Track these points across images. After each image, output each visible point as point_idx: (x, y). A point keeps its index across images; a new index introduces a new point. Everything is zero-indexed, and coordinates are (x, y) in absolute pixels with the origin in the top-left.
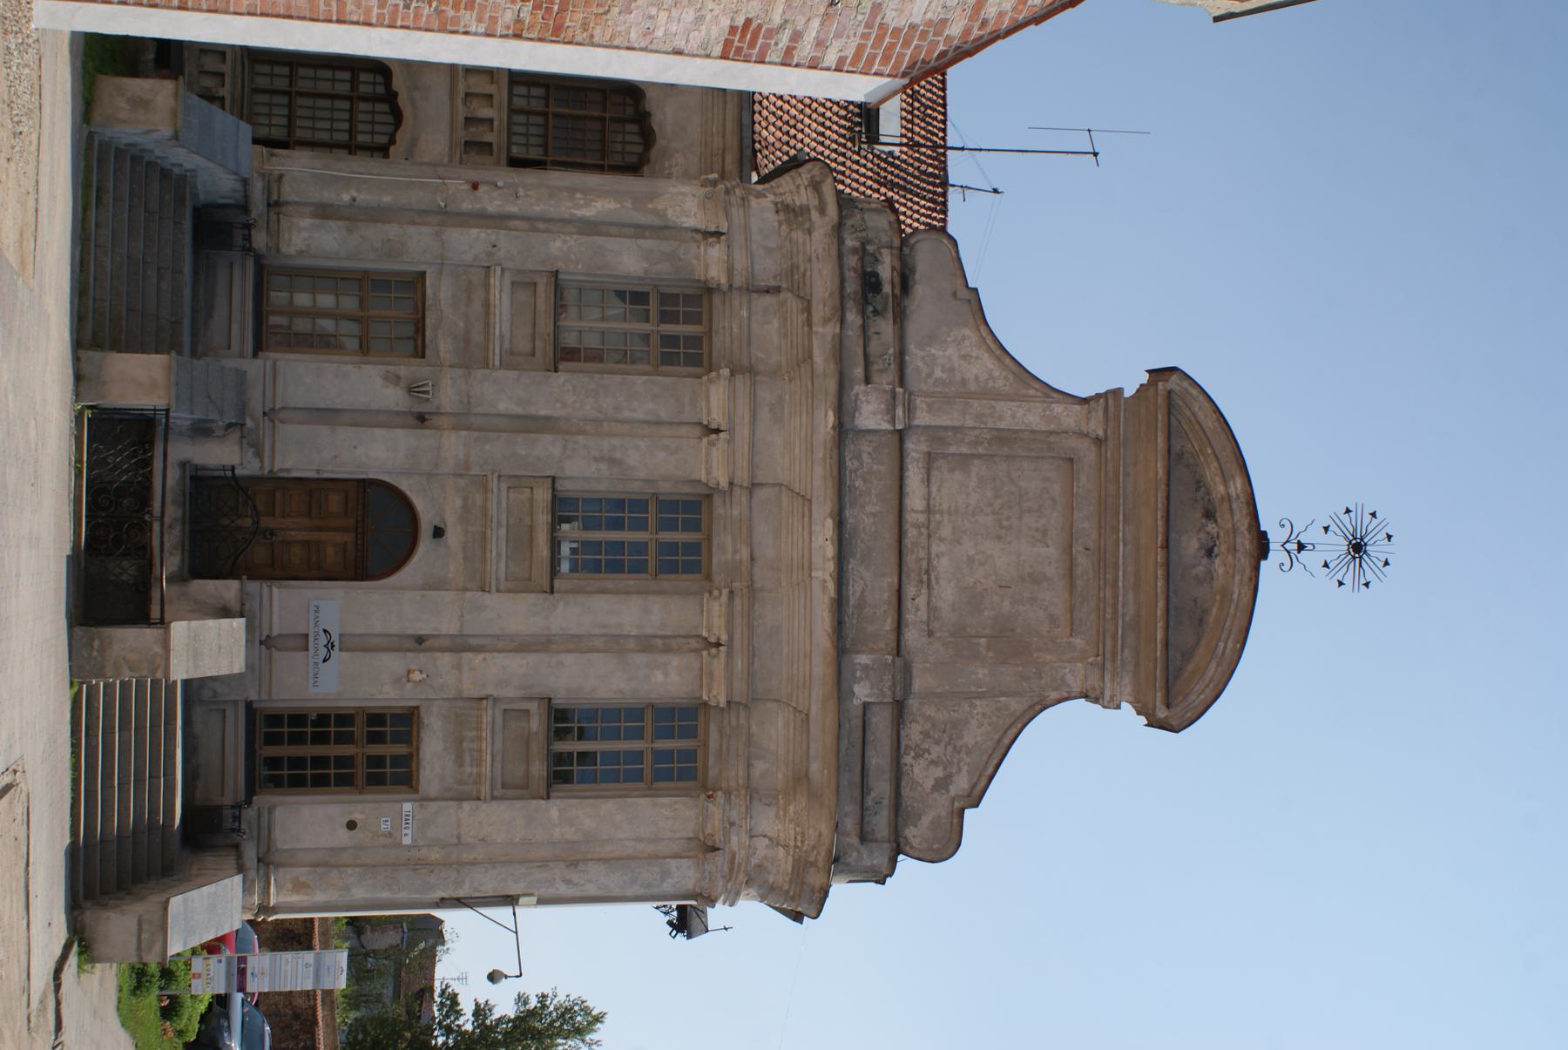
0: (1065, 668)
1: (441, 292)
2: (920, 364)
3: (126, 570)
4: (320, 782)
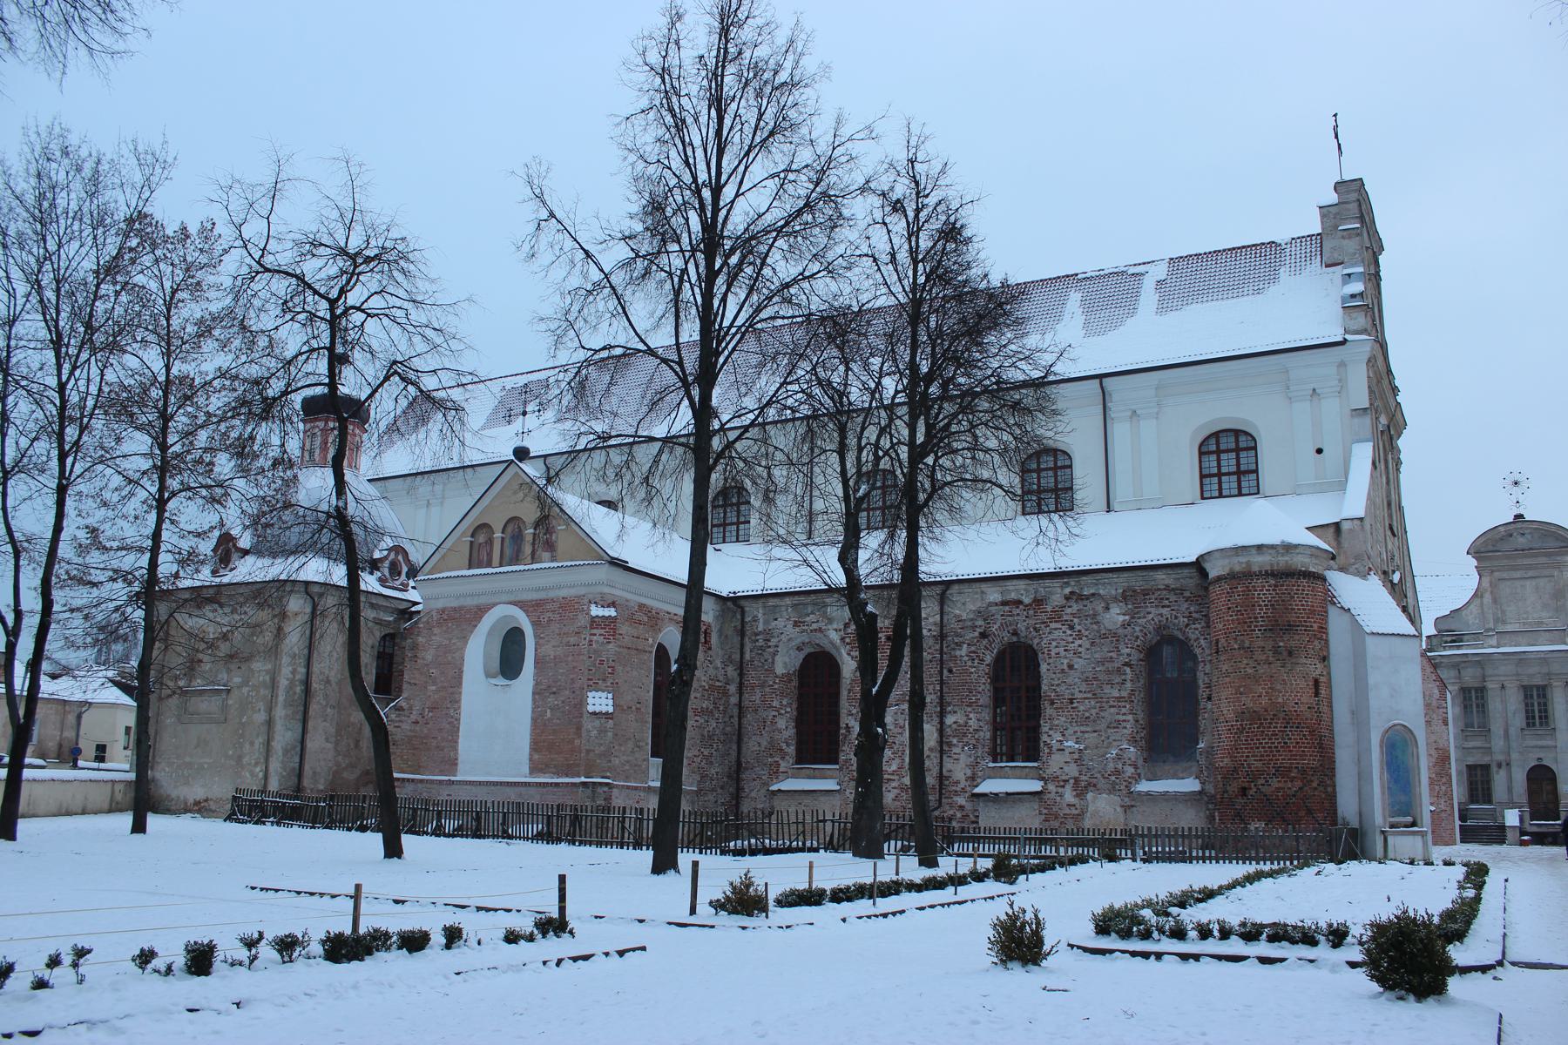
1: (1471, 761)
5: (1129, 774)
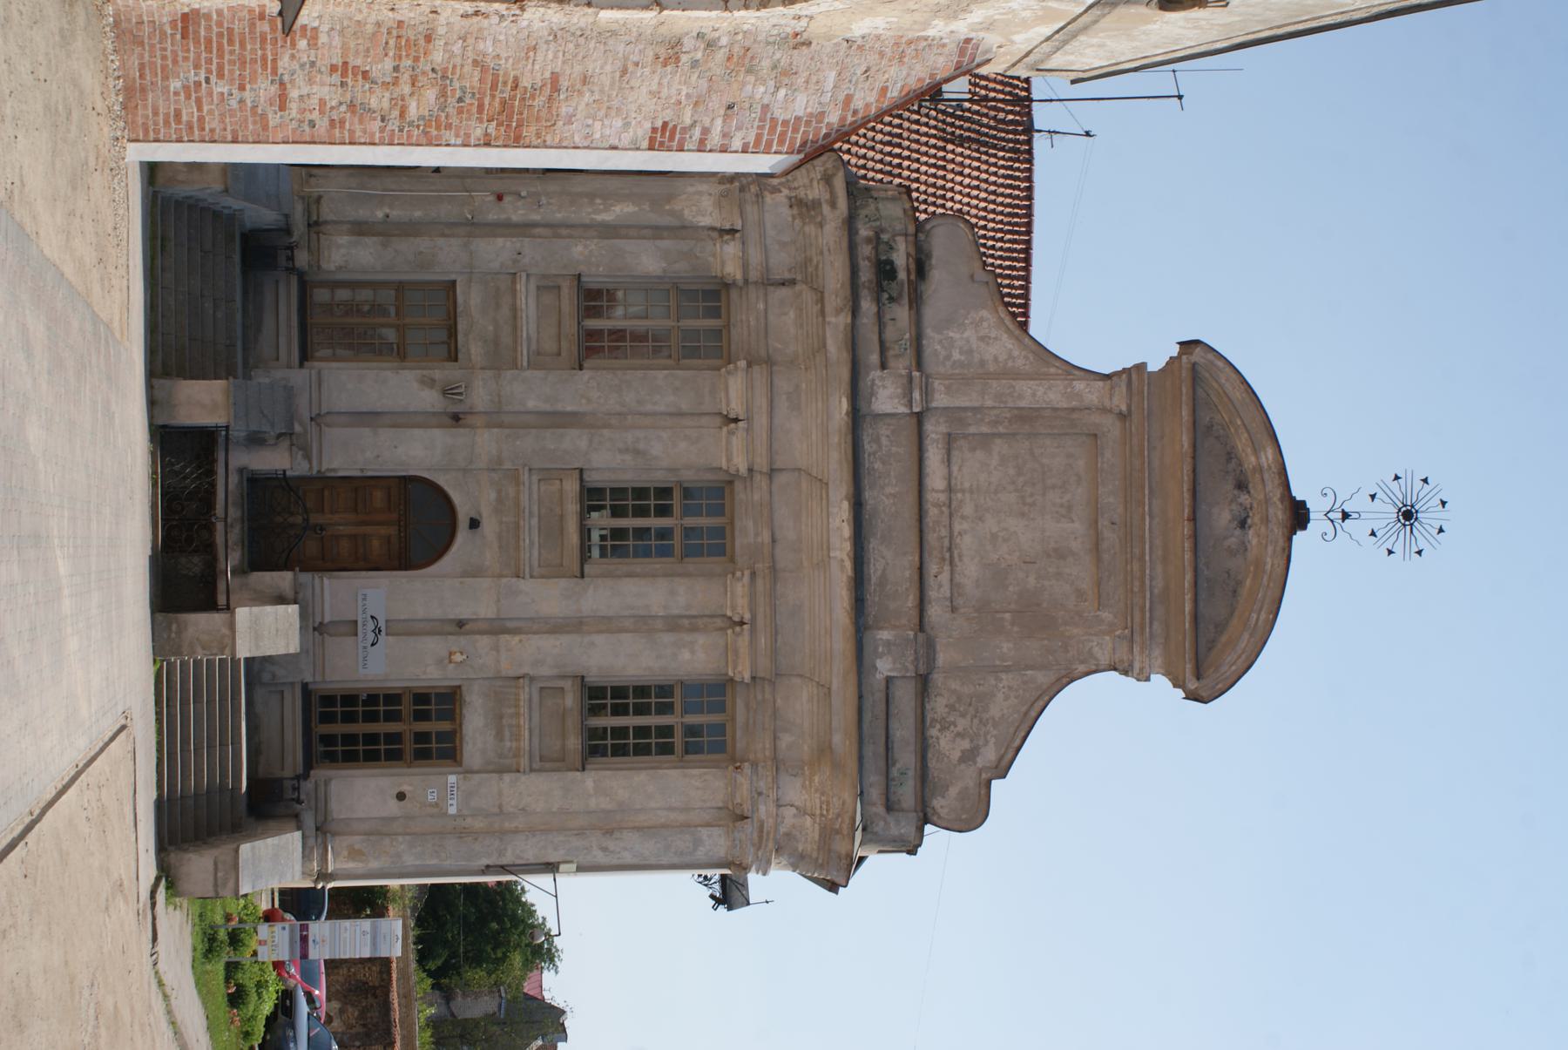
0: (1093, 641)
1: (471, 299)
2: (938, 347)
3: (195, 564)
4: (372, 757)
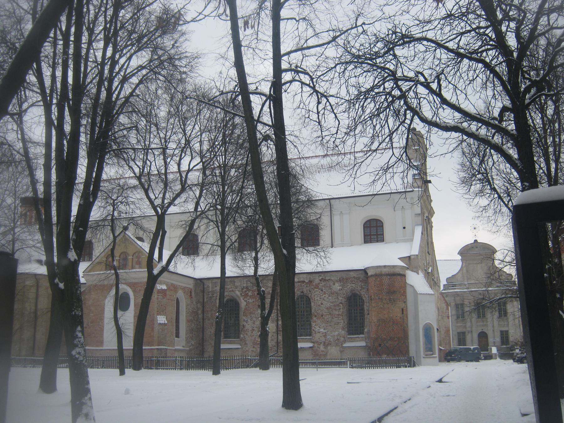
1: (459, 330)
5: (342, 340)
